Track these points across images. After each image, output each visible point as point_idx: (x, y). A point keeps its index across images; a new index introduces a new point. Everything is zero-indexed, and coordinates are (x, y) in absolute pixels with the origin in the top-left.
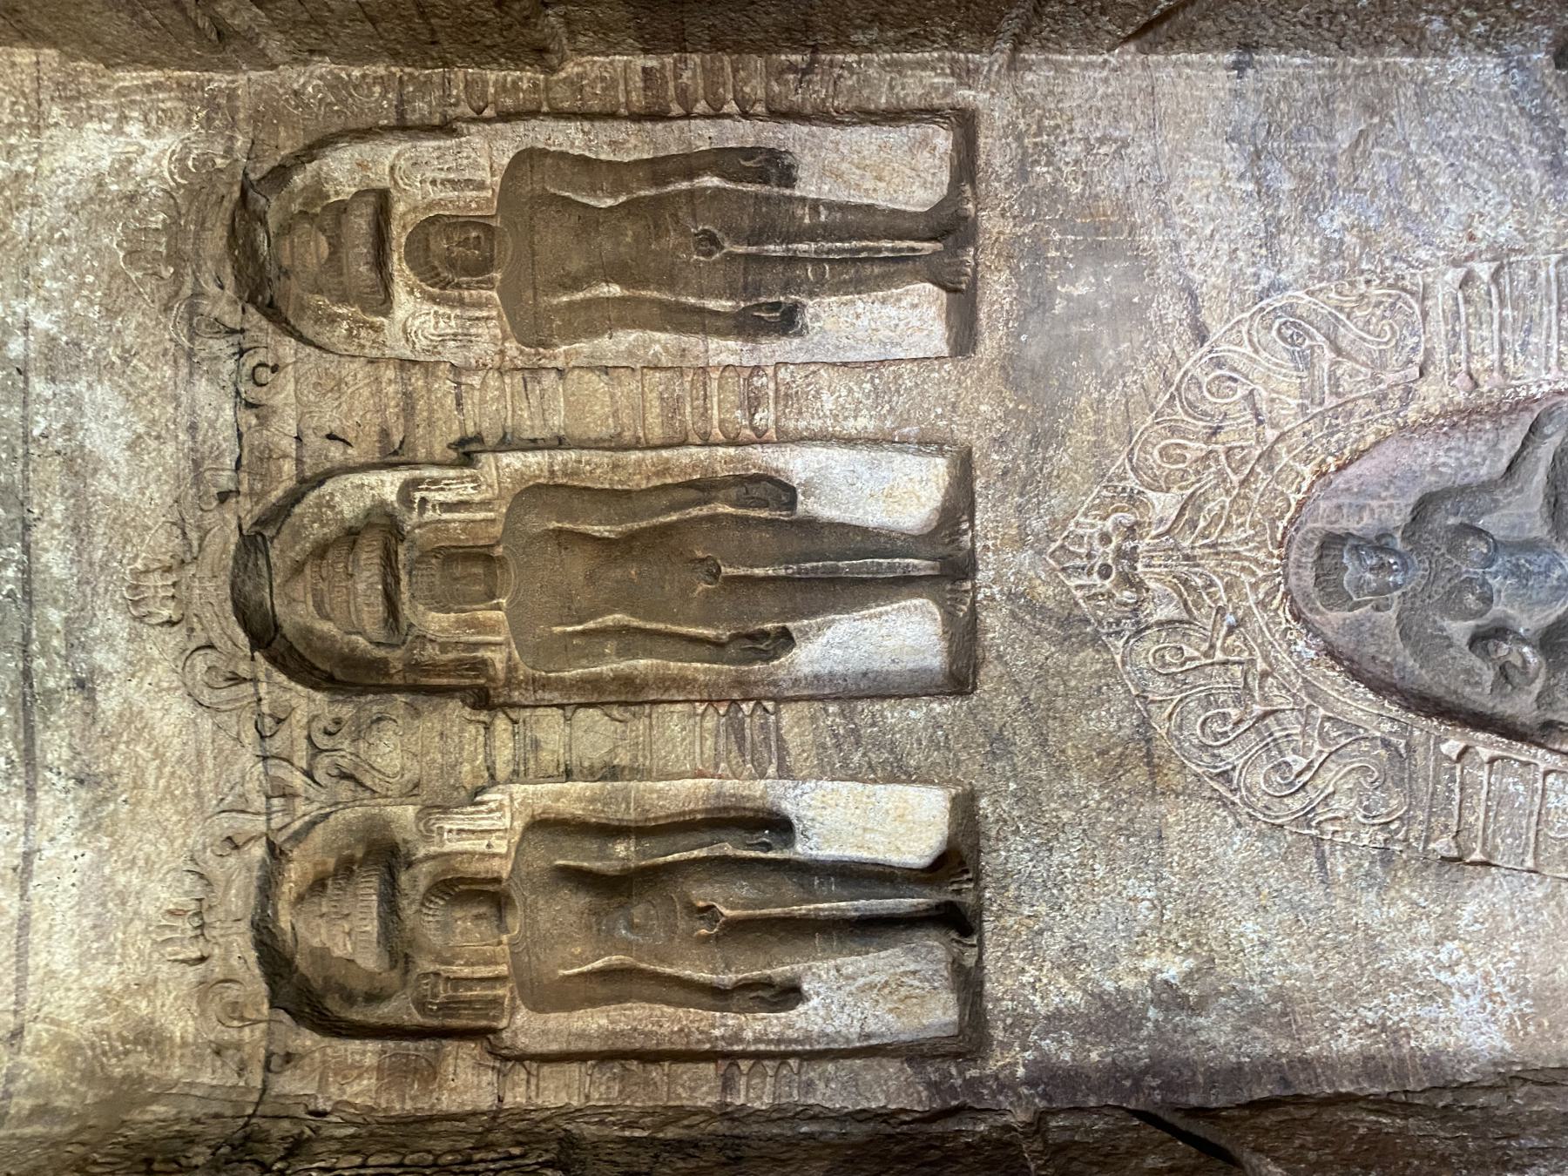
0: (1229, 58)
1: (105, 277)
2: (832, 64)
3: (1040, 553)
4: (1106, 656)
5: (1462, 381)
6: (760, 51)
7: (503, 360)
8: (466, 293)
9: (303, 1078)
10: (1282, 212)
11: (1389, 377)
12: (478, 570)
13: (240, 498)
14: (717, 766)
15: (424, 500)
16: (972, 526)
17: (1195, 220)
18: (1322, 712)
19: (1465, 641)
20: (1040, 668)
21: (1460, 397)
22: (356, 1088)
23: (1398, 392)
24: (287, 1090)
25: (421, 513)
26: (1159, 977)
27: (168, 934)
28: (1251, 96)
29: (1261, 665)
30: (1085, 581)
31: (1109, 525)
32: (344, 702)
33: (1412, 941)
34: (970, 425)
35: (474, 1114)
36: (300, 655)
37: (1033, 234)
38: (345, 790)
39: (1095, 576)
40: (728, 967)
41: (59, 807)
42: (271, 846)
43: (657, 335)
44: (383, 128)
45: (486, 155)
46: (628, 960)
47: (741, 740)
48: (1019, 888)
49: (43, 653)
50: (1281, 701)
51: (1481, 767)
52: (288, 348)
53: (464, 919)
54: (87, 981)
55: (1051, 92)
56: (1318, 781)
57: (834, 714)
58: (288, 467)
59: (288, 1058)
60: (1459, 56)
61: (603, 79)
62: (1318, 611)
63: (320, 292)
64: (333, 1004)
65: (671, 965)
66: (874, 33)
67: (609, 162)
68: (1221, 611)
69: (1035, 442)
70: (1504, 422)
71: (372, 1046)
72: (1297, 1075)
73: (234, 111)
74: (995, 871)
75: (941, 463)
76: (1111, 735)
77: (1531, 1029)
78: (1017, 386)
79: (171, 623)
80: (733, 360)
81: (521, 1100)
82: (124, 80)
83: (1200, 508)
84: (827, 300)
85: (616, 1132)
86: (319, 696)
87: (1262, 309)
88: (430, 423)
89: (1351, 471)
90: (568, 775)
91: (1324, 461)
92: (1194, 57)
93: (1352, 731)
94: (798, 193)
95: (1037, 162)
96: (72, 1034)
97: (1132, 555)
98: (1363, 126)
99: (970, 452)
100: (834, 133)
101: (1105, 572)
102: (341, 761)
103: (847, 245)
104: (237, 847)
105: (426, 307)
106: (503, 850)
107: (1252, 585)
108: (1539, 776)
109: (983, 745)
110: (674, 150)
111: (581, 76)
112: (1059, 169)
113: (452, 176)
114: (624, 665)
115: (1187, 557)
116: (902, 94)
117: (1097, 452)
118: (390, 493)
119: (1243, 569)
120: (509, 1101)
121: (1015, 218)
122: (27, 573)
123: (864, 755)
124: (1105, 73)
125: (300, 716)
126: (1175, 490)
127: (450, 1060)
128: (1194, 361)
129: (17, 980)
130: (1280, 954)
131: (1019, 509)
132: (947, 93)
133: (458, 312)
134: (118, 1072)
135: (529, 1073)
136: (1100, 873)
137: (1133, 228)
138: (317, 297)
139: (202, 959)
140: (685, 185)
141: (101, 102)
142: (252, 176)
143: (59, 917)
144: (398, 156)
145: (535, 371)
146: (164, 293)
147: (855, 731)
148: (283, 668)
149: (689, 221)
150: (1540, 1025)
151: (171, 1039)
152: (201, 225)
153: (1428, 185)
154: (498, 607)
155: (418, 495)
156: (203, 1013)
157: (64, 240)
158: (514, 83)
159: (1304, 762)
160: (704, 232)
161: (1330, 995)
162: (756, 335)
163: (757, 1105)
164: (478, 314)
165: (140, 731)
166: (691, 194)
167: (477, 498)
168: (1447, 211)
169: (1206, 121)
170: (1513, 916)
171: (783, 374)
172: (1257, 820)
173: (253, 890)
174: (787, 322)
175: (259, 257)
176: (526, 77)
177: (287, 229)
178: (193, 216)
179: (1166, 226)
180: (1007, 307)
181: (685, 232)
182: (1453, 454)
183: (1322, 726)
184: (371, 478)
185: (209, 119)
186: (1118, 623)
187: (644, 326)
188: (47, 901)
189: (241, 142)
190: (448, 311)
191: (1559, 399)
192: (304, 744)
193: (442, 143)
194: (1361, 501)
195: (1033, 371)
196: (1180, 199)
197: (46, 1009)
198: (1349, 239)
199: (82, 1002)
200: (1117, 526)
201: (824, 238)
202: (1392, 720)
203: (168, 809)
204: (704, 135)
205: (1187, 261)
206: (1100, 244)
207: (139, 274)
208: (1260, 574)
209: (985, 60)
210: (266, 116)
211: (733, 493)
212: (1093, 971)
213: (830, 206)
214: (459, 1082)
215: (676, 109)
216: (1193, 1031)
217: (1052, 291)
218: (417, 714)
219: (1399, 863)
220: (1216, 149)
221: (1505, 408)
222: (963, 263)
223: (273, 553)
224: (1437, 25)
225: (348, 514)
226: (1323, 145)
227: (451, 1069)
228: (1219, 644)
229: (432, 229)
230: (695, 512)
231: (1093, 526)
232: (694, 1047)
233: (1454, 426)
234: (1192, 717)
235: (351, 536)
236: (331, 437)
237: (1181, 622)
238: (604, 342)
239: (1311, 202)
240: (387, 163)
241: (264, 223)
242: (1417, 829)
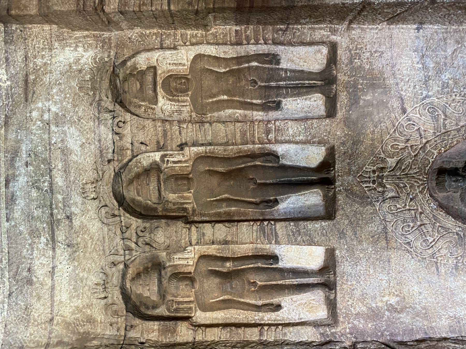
0: (415, 26)
1: (73, 95)
3: (355, 177)
4: (374, 208)
6: (271, 25)
7: (191, 118)
8: (180, 98)
9: (136, 333)
10: (430, 74)
12: (185, 182)
13: (115, 162)
14: (257, 241)
15: (168, 161)
16: (334, 169)
17: (403, 76)
18: (438, 224)
20: (355, 212)
22: (152, 335)
24: (132, 336)
25: (167, 164)
26: (388, 302)
27: (95, 291)
28: (421, 38)
29: (420, 210)
30: (368, 185)
32: (147, 222)
33: (464, 292)
34: (334, 138)
35: (187, 343)
36: (132, 207)
37: (354, 81)
38: (147, 248)
39: (371, 184)
40: (260, 299)
41: (62, 253)
42: (125, 264)
43: (238, 111)
44: (156, 49)
47: (264, 233)
49: (56, 208)
50: (426, 221)
52: (128, 116)
53: (182, 285)
54: (72, 304)
55: (360, 37)
56: (437, 245)
57: (292, 226)
58: (129, 152)
59: (132, 326)
61: (223, 33)
63: (136, 98)
64: (143, 309)
65: (243, 299)
66: (308, 20)
67: (224, 58)
69: (353, 144)
71: (156, 323)
72: (429, 331)
73: (110, 44)
74: (340, 272)
76: (375, 231)
79: (94, 199)
80: (260, 118)
81: (201, 339)
82: (77, 34)
83: (403, 164)
84: (289, 99)
86: (139, 220)
87: (423, 103)
88: (172, 139)
90: (213, 243)
91: (441, 149)
92: (404, 26)
93: (447, 230)
94: (280, 67)
95: (356, 59)
96: (68, 320)
98: (456, 48)
99: (334, 146)
100: (292, 48)
101: (374, 182)
102: (146, 240)
104: (115, 265)
105: (168, 102)
106: (192, 264)
109: (337, 235)
110: (243, 54)
111: (216, 32)
112: (362, 61)
113: (175, 62)
114: (227, 209)
115: (398, 178)
116: (314, 37)
117: (372, 147)
118: (158, 158)
120: (197, 339)
121: (348, 75)
122: (51, 184)
123: (301, 238)
124: (377, 31)
125: (134, 226)
126: (395, 158)
127: (179, 327)
128: (402, 119)
129: (51, 304)
130: (424, 296)
131: (349, 164)
132: (328, 37)
133: (177, 104)
134: (82, 331)
135: (203, 331)
136: (371, 272)
137: (384, 79)
138: (135, 99)
139: (105, 298)
140: (247, 65)
141: (70, 41)
142: (116, 64)
143: (63, 286)
144: (159, 56)
145: (202, 122)
146: (90, 100)
148: (128, 212)
149: (248, 76)
151: (97, 321)
152: (101, 79)
154: (191, 192)
155: (166, 159)
156: (106, 314)
157: (60, 84)
158: (196, 35)
159: (432, 239)
160: (253, 80)
161: (439, 308)
162: (268, 111)
163: (270, 340)
164: (183, 104)
165: (86, 231)
166: (249, 68)
167: (183, 160)
169: (407, 46)
171: (277, 123)
172: (418, 256)
173: (120, 277)
175: (119, 87)
176: (200, 32)
177: (125, 80)
178: (99, 76)
179: (394, 78)
180: (346, 103)
183: (438, 229)
184: (152, 154)
185: (103, 46)
187: (234, 108)
188: (59, 281)
190: (174, 103)
192: (135, 235)
193: (172, 52)
195: (353, 122)
196: (399, 70)
197: (60, 312)
199: (71, 310)
201: (288, 80)
202: (460, 227)
203: (94, 254)
204: (252, 49)
205: (400, 89)
207: (83, 94)
208: (420, 183)
209: (340, 27)
210: (120, 45)
211: (262, 159)
212: (369, 301)
213: (291, 71)
214: (182, 334)
215: (245, 42)
216: (399, 319)
217: (359, 98)
218: (169, 225)
219: (461, 269)
223: (123, 177)
226: (443, 53)
227: (180, 330)
228: (408, 204)
229: (171, 80)
231: (370, 169)
232: (250, 322)
234: (399, 226)
235: (147, 171)
236: (142, 143)
237: (396, 197)
238: (222, 113)
239: (439, 71)
240: (156, 58)
241: (119, 77)
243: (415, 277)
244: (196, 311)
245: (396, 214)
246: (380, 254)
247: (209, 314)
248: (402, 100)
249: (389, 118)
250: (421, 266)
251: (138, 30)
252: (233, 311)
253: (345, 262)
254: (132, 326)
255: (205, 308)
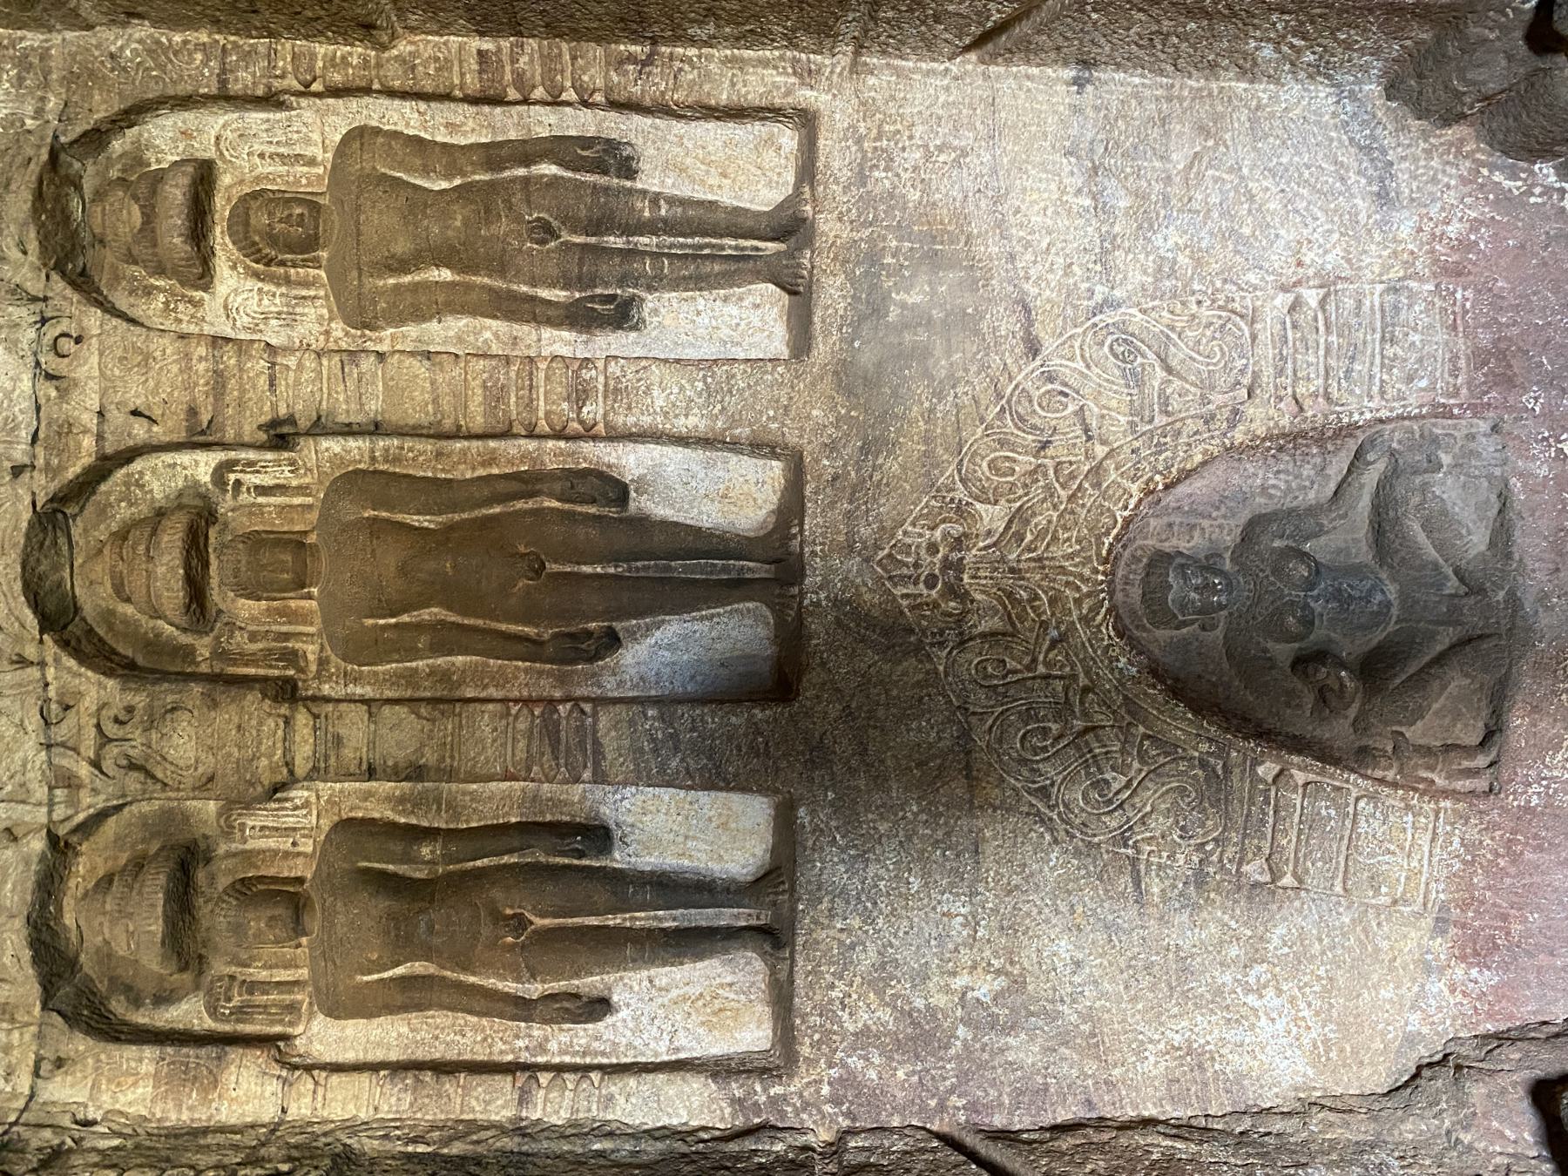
0: (1069, 73)
2: (671, 57)
4: (928, 666)
5: (1287, 405)
6: (599, 40)
7: (327, 341)
9: (72, 1086)
10: (1117, 229)
11: (1218, 399)
13: (35, 473)
14: (529, 770)
15: (238, 483)
16: (802, 531)
17: (1033, 232)
18: (1141, 729)
19: (1288, 663)
20: (863, 676)
21: (1285, 422)
22: (130, 1097)
23: (1226, 413)
25: (235, 497)
26: (970, 995)
28: (1090, 113)
29: (1083, 681)
30: (910, 590)
31: (938, 534)
32: (137, 690)
33: (1222, 964)
34: (802, 429)
35: (253, 1126)
36: (101, 639)
38: (133, 782)
39: (921, 586)
40: (533, 976)
42: (53, 839)
43: (488, 321)
45: (319, 129)
46: (432, 969)
47: (555, 743)
48: (832, 901)
50: (1099, 719)
51: (1295, 790)
52: (94, 319)
53: (258, 919)
55: (893, 98)
56: (1137, 800)
57: (653, 718)
58: (88, 442)
60: (1293, 83)
61: (437, 59)
62: (1145, 629)
63: (136, 263)
64: (118, 1007)
65: (474, 974)
66: (711, 28)
67: (444, 145)
68: (1044, 625)
69: (865, 450)
70: (1330, 447)
71: (149, 1052)
72: (1101, 1097)
74: (809, 882)
75: (777, 466)
77: (1333, 1055)
78: (849, 392)
80: (565, 351)
81: (306, 1112)
83: (1028, 522)
84: (667, 295)
85: (399, 1147)
86: (111, 683)
88: (241, 404)
89: (1181, 489)
90: (371, 773)
91: (1151, 479)
92: (1035, 71)
94: (639, 185)
97: (959, 567)
98: (1198, 149)
99: (801, 457)
100: (678, 127)
101: (931, 582)
102: (131, 752)
103: (689, 241)
104: (15, 839)
105: (251, 283)
106: (309, 849)
107: (1075, 600)
108: (1352, 801)
109: (803, 753)
110: (513, 135)
111: (413, 55)
112: (898, 175)
115: (1012, 570)
116: (743, 90)
118: (204, 475)
119: (1068, 584)
123: (682, 760)
124: (946, 82)
125: (89, 703)
126: (1003, 502)
127: (233, 1068)
128: (1027, 374)
130: (1091, 974)
131: (848, 515)
132: (788, 93)
133: (283, 290)
135: (316, 1083)
138: (134, 268)
140: (521, 172)
142: (63, 139)
147: (674, 737)
148: (78, 654)
149: (524, 209)
150: (1342, 1050)
153: (1259, 210)
154: (309, 597)
155: (232, 477)
158: (343, 58)
159: (1124, 779)
160: (538, 219)
161: (1138, 1017)
162: (589, 327)
163: (554, 1120)
164: (304, 293)
166: (526, 180)
167: (294, 483)
168: (1277, 236)
169: (1045, 134)
170: (1320, 940)
171: (613, 368)
172: (1073, 837)
174: (622, 316)
176: (356, 52)
177: (99, 195)
179: (1002, 237)
180: (841, 312)
181: (519, 219)
182: (1282, 476)
184: (184, 458)
185: (20, 79)
186: (941, 633)
187: (474, 312)
189: (53, 103)
190: (273, 288)
191: (1380, 427)
192: (93, 732)
193: (271, 116)
194: (1193, 521)
195: (865, 378)
196: (1017, 211)
198: (1183, 259)
200: (946, 535)
201: (665, 233)
202: (1210, 740)
204: (545, 122)
206: (936, 252)
208: (1085, 589)
209: (827, 62)
210: (81, 77)
211: (558, 487)
213: (672, 201)
214: (240, 1092)
217: (886, 297)
218: (214, 705)
220: (1054, 163)
221: (1330, 433)
222: (799, 265)
223: (76, 532)
224: (1267, 51)
225: (158, 496)
226: (1157, 164)
227: (233, 1078)
228: (1041, 658)
229: (254, 204)
230: (520, 505)
231: (921, 535)
232: (496, 1058)
233: (1281, 449)
236: (136, 413)
237: (1004, 634)
238: (433, 326)
239: (1146, 223)
240: (213, 133)
241: (78, 188)
242: (1231, 851)
243: (1063, 907)
244: (311, 1016)
245: (1001, 689)
246: (946, 823)
247: (354, 1029)
248: (1027, 310)
249: (984, 367)
250: (1083, 872)
251: (142, 31)
252: (441, 1018)
253: (828, 849)
254: (59, 1063)
255: (339, 1007)
